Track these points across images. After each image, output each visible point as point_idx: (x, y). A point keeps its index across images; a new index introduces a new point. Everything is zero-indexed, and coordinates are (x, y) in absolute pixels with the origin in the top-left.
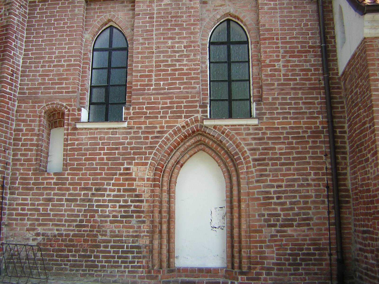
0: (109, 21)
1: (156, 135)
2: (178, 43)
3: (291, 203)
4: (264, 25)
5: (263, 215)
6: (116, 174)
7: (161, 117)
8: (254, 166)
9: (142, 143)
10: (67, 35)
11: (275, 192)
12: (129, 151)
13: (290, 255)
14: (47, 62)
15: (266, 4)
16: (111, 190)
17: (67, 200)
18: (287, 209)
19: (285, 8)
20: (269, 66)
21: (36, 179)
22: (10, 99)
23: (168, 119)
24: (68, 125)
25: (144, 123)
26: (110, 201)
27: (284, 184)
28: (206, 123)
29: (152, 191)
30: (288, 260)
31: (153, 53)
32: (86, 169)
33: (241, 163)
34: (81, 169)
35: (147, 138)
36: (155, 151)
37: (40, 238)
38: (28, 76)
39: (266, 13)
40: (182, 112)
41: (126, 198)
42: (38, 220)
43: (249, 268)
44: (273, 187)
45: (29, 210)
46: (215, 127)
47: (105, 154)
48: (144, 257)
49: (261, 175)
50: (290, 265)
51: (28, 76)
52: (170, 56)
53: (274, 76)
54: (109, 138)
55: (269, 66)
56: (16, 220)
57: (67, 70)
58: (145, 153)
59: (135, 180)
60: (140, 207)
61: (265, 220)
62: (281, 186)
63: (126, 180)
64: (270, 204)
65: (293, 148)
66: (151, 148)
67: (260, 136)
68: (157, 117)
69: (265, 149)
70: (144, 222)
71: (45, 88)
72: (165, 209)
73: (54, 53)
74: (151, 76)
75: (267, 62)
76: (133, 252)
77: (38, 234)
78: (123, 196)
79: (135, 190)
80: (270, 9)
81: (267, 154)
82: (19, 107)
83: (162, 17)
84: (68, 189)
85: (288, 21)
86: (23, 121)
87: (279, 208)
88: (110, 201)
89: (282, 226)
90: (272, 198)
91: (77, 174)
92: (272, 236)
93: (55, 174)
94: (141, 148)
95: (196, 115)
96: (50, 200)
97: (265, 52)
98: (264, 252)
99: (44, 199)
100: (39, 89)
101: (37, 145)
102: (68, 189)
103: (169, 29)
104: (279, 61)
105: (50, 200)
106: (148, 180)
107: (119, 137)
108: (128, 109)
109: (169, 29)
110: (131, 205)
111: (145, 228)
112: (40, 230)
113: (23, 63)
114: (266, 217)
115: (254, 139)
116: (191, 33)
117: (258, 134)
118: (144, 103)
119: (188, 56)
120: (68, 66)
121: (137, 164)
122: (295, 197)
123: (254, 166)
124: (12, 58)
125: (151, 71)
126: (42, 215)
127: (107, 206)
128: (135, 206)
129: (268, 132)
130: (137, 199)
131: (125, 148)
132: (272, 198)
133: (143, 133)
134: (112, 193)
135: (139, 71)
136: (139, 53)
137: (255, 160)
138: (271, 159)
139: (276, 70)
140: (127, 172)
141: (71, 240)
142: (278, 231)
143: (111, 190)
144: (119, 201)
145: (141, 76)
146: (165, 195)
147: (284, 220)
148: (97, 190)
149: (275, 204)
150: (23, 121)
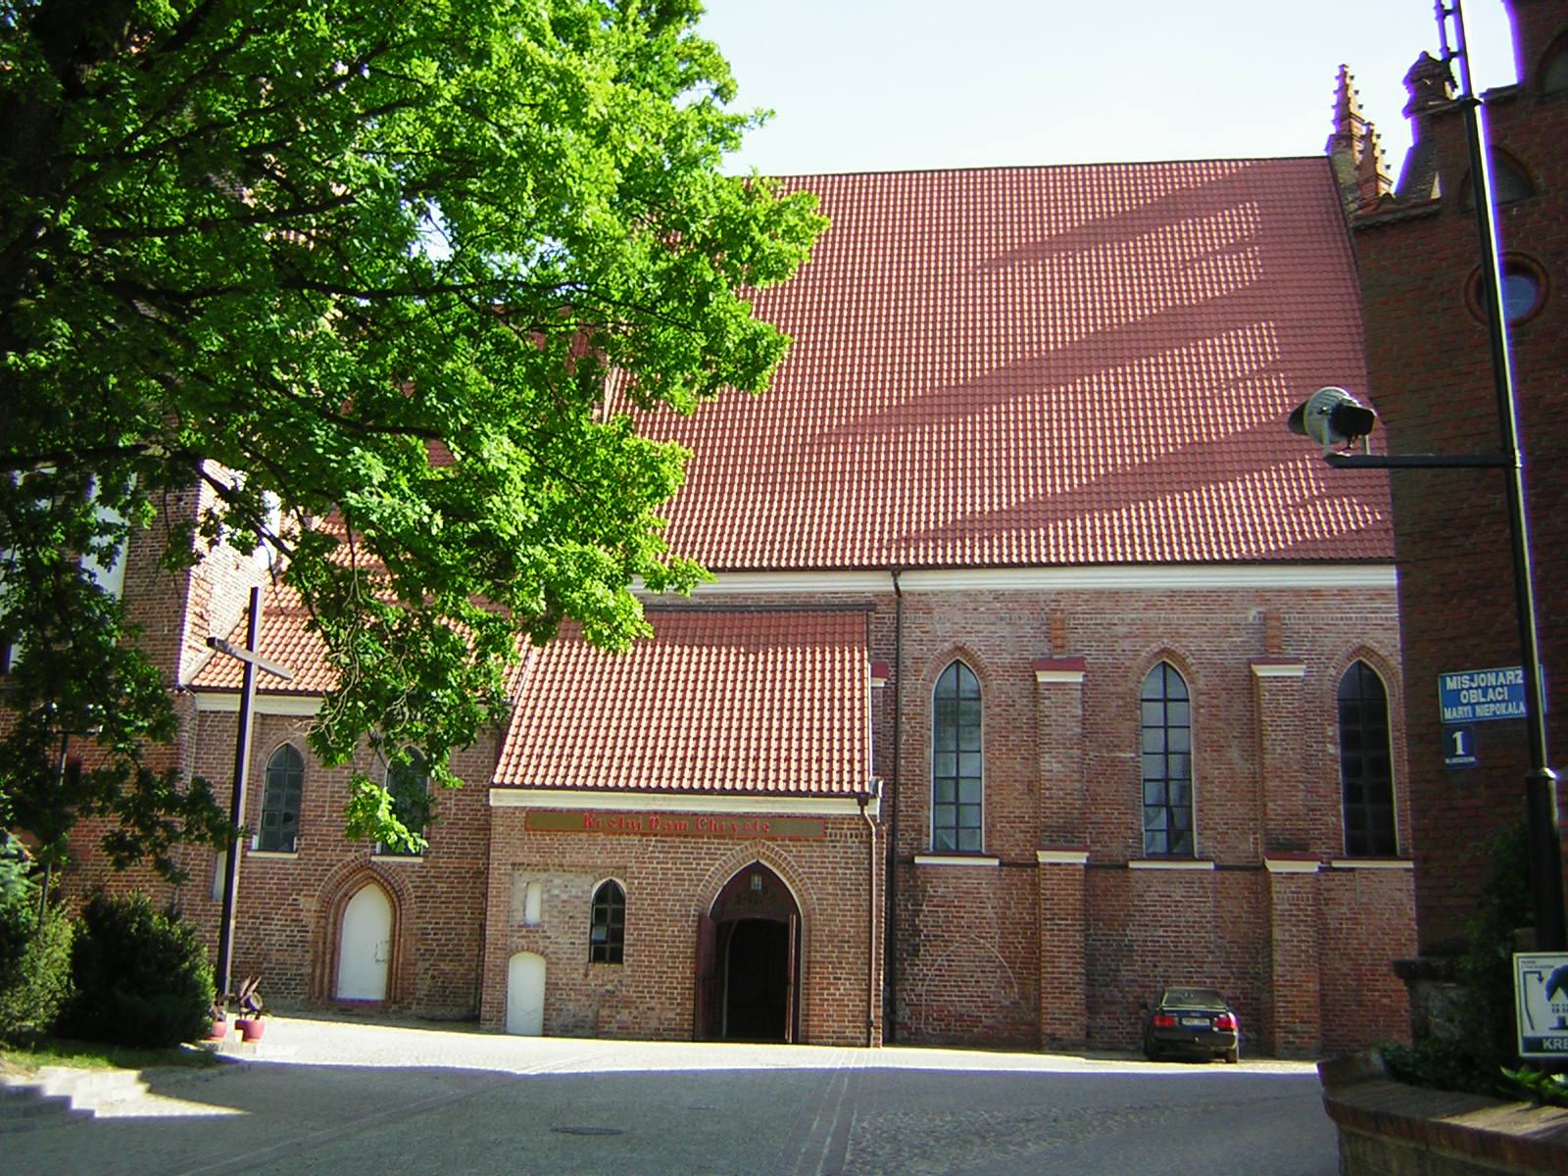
28: (374, 859)
72: (329, 938)
75: (440, 799)
111: (309, 957)
140: (295, 904)
146: (330, 928)
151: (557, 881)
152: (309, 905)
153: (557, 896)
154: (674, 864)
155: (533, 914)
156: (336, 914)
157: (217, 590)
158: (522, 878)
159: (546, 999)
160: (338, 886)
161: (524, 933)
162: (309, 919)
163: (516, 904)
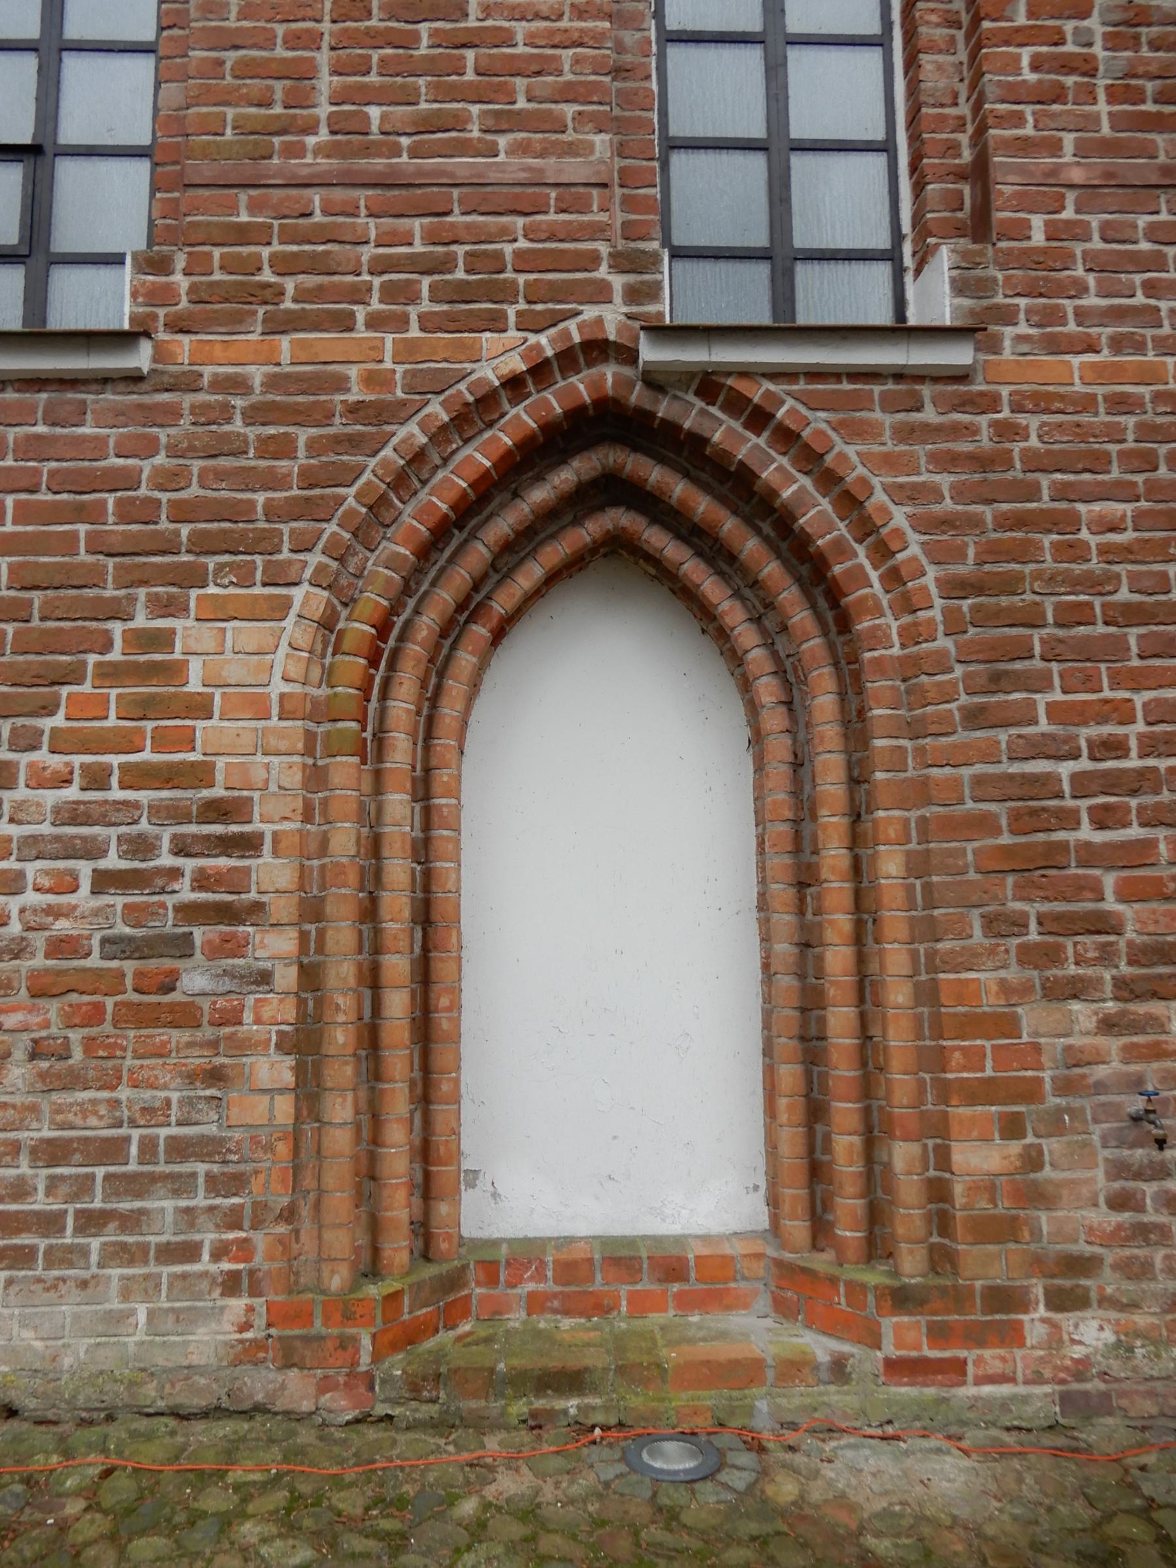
1: (338, 426)
5: (1019, 924)
6: (74, 675)
7: (374, 322)
8: (954, 626)
9: (250, 480)
11: (1082, 785)
12: (164, 525)
16: (42, 780)
23: (414, 332)
26: (34, 848)
29: (316, 778)
35: (282, 448)
36: (332, 528)
40: (507, 293)
41: (144, 825)
49: (997, 681)
53: (1059, 95)
58: (266, 544)
59: (201, 708)
60: (236, 881)
62: (1116, 747)
63: (143, 709)
64: (1055, 855)
67: (985, 441)
68: (345, 323)
69: (1020, 521)
74: (303, 74)
76: (181, 1185)
79: (201, 774)
81: (1024, 552)
87: (1109, 881)
88: (34, 848)
90: (1070, 820)
95: (590, 312)
107: (101, 441)
110: (175, 873)
114: (1033, 936)
115: (946, 462)
117: (971, 431)
121: (219, 613)
128: (202, 881)
129: (1033, 422)
130: (218, 829)
131: (146, 512)
133: (254, 415)
134: (51, 797)
137: (955, 588)
139: (1067, 65)
144: (92, 851)
145: (245, 70)
149: (1090, 855)
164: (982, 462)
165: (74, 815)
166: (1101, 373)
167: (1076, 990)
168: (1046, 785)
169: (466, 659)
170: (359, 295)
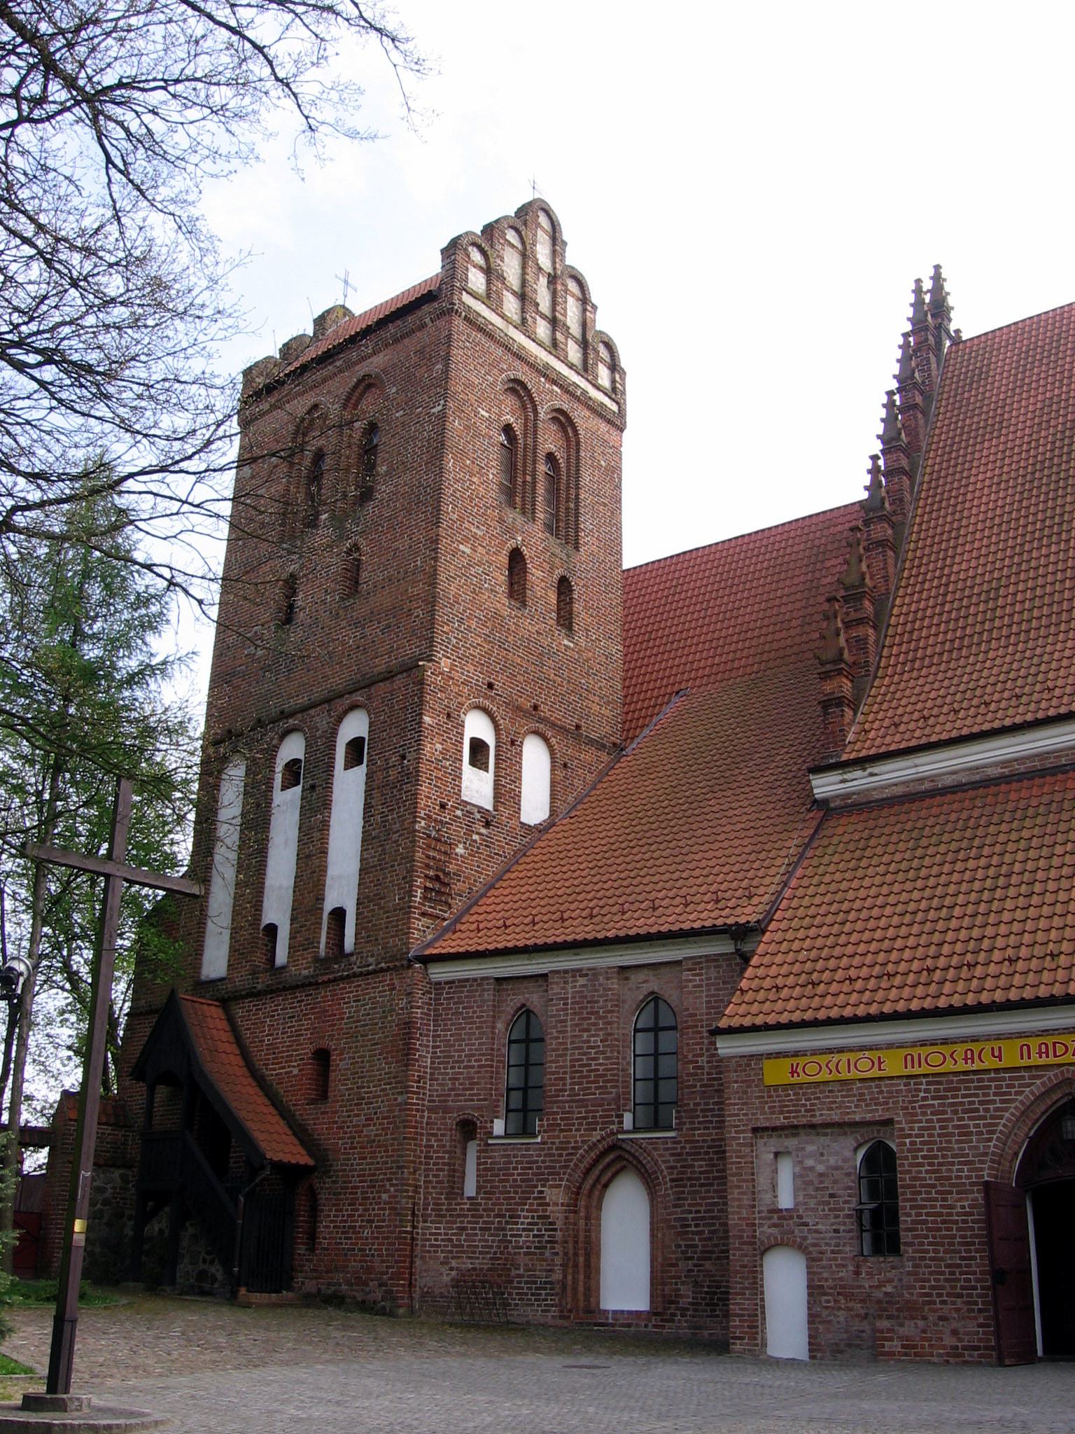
0: (524, 1005)
2: (593, 1036)
3: (710, 1232)
4: (687, 1009)
5: (680, 1246)
8: (672, 1187)
10: (477, 1028)
11: (693, 1219)
13: (706, 1293)
14: (457, 1062)
15: (691, 981)
16: (526, 1217)
17: (481, 1229)
18: (705, 1239)
19: (712, 984)
20: (692, 1062)
21: (449, 1204)
22: (417, 1110)
24: (481, 1139)
25: (558, 1137)
26: (524, 1230)
27: (702, 1209)
29: (566, 1218)
30: (704, 1299)
31: (567, 1049)
32: (501, 1193)
33: (659, 1184)
34: (494, 1193)
35: (561, 1155)
37: (453, 1273)
38: (436, 1079)
39: (690, 992)
42: (451, 1252)
43: (665, 1309)
44: (691, 1212)
45: (443, 1240)
46: (631, 1140)
47: (519, 1174)
48: (557, 1294)
49: (679, 1199)
50: (707, 1305)
51: (436, 1079)
52: (586, 1054)
53: (697, 1074)
54: (523, 1156)
55: (692, 1062)
56: (429, 1252)
57: (478, 1072)
58: (559, 1174)
59: (548, 1205)
60: (554, 1236)
61: (683, 1252)
63: (539, 1205)
65: (714, 1165)
66: (566, 1167)
70: (557, 1254)
71: (456, 1095)
73: (463, 1051)
74: (564, 1079)
75: (690, 1057)
76: (545, 1289)
77: (452, 1269)
78: (536, 1224)
79: (548, 1217)
80: (695, 986)
82: (429, 1118)
83: (577, 1003)
84: (482, 1216)
85: (716, 1002)
86: (433, 1135)
88: (524, 1230)
89: (699, 1259)
90: (689, 1226)
91: (490, 1199)
92: (689, 1271)
93: (469, 1198)
94: (554, 1168)
96: (463, 1229)
97: (688, 1044)
98: (679, 1290)
99: (458, 1228)
100: (449, 1095)
101: (449, 1164)
102: (482, 1216)
103: (584, 1019)
104: (702, 1055)
105: (463, 1229)
106: (562, 1205)
108: (541, 1120)
109: (584, 1019)
111: (558, 1260)
112: (454, 1263)
113: (432, 1063)
116: (609, 1023)
118: (557, 1113)
119: (603, 1053)
120: (479, 1066)
121: (552, 1186)
122: (714, 1224)
123: (672, 1187)
124: (417, 1060)
125: (565, 1073)
126: (456, 1246)
127: (520, 1236)
132: (689, 1226)
135: (553, 1073)
136: (554, 1050)
137: (672, 1180)
138: (690, 1179)
141: (485, 1275)
142: (695, 1265)
143: (526, 1217)
144: (532, 1230)
145: (556, 1079)
146: (582, 1222)
147: (702, 1252)
148: (511, 1217)
149: (693, 1233)
150: (433, 1135)
151: (811, 1148)
152: (556, 1196)
153: (811, 1169)
154: (955, 1112)
155: (786, 1200)
156: (587, 1208)
157: (460, 850)
158: (766, 1149)
159: (809, 1309)
160: (587, 1172)
161: (775, 1220)
162: (557, 1213)
163: (763, 1181)
164: (679, 1155)
165: (529, 1224)
166: (700, 1135)
167: (691, 1258)
168: (686, 1219)
169: (597, 1193)
170: (574, 1124)
